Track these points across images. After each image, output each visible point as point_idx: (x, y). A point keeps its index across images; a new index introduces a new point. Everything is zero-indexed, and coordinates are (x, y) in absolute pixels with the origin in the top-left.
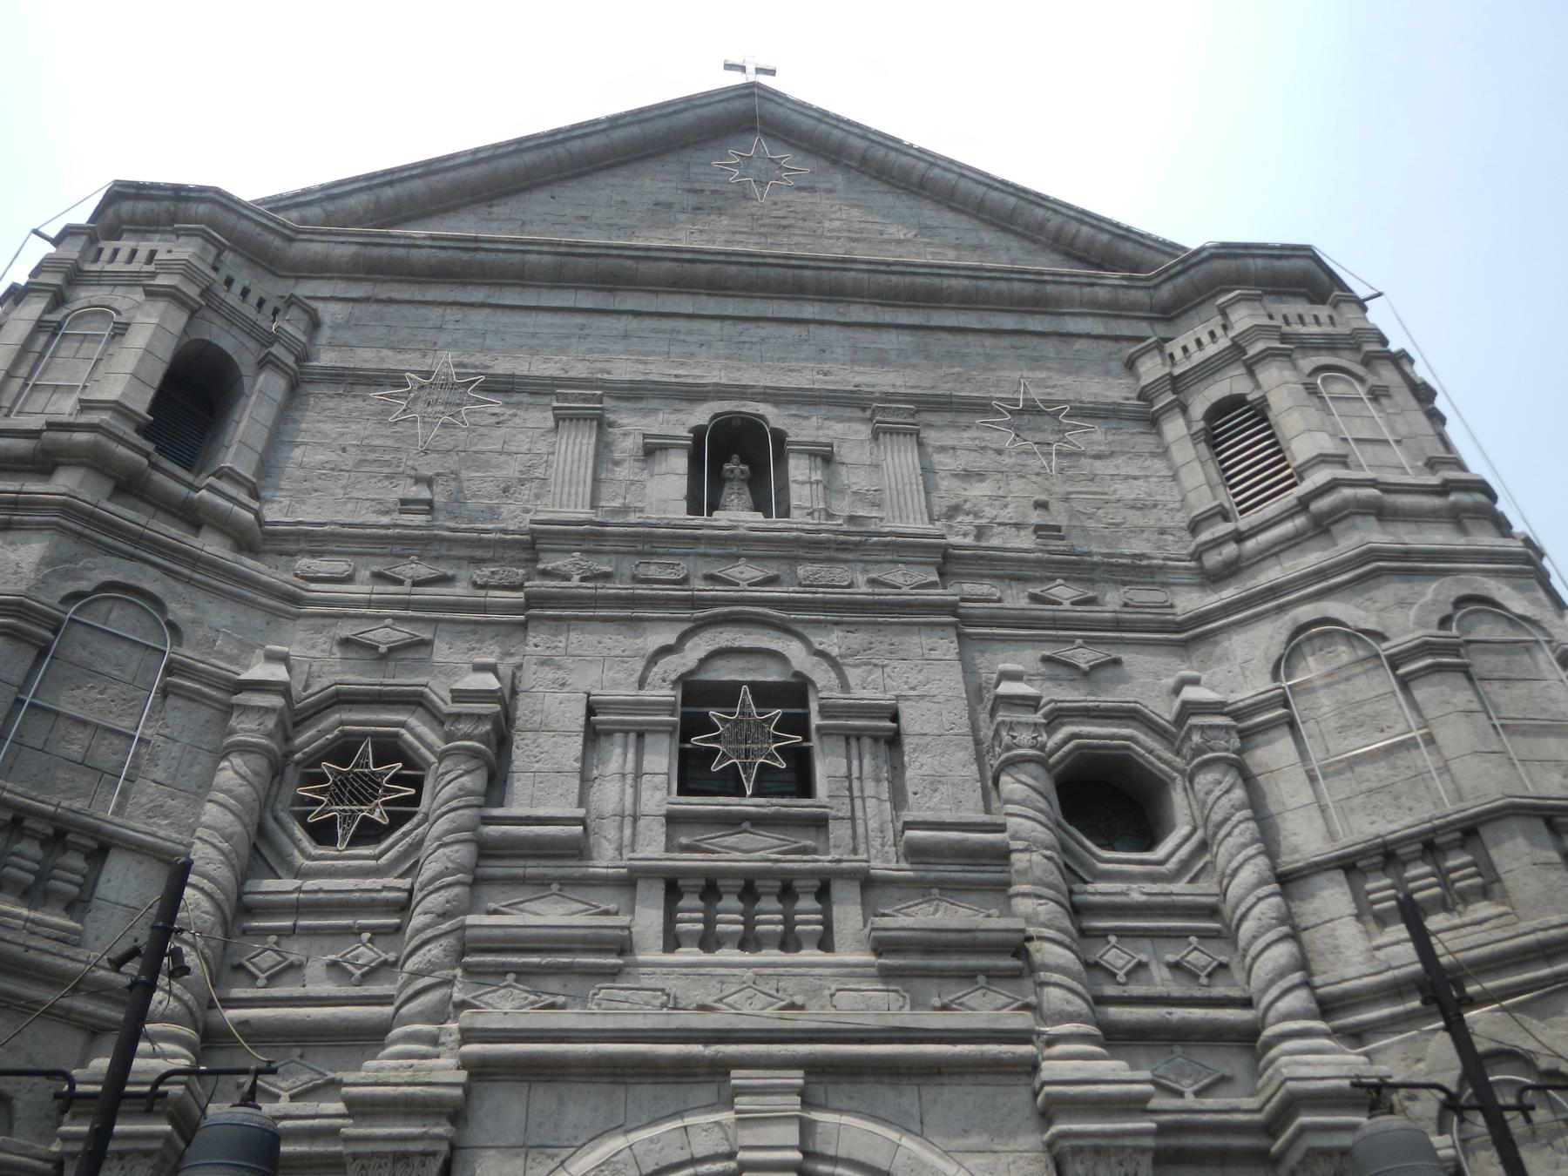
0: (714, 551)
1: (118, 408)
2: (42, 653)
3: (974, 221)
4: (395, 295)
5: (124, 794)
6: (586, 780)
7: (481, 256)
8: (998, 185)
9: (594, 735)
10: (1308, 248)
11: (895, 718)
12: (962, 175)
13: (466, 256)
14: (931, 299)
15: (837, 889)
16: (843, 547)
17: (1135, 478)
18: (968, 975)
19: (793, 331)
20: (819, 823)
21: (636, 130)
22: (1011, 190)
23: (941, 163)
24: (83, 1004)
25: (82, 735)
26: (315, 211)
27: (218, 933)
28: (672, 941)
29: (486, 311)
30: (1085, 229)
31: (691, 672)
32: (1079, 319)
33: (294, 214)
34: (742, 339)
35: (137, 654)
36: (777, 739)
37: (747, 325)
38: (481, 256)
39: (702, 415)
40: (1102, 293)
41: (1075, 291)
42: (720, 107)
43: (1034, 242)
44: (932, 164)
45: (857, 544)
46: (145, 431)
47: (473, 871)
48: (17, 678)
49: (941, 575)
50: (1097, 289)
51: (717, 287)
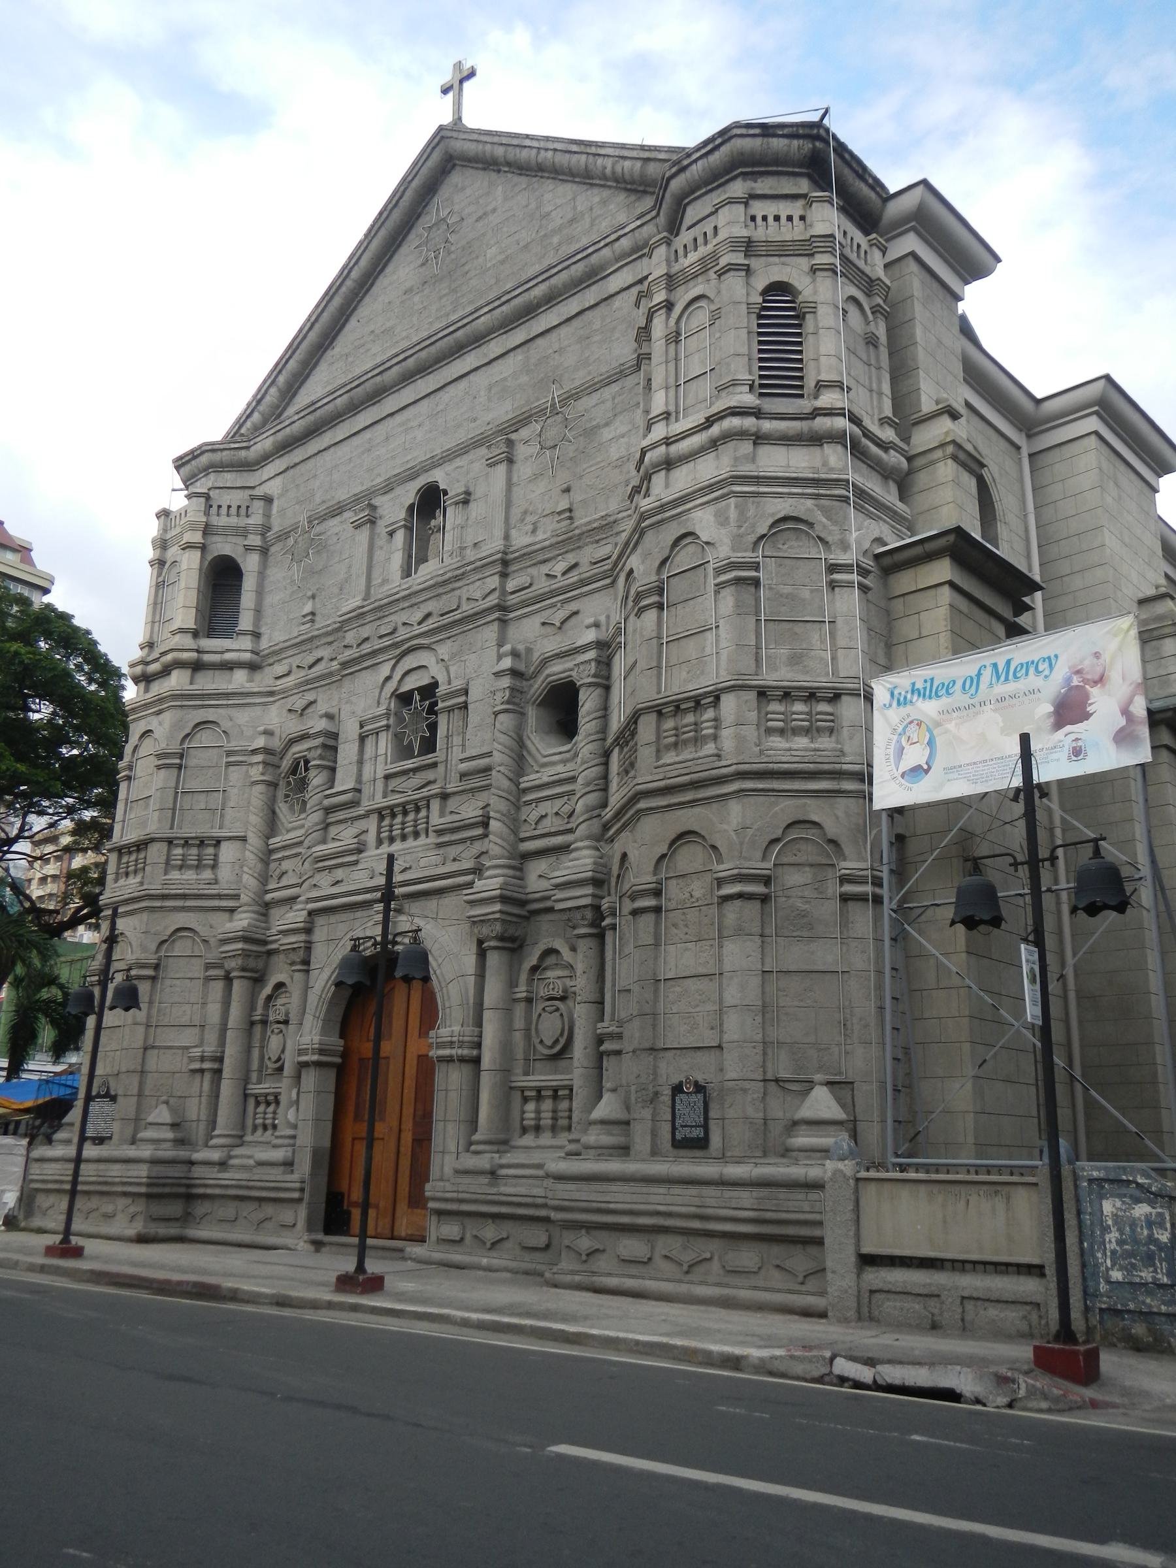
0: (407, 604)
1: (182, 631)
2: (180, 767)
3: (575, 186)
4: (297, 460)
5: (222, 816)
6: (360, 762)
7: (318, 413)
8: (574, 148)
9: (362, 739)
10: (737, 125)
11: (466, 692)
12: (555, 150)
13: (311, 418)
14: (529, 311)
15: (432, 802)
16: (457, 578)
17: (623, 436)
18: (463, 841)
19: (463, 384)
20: (434, 765)
21: (383, 233)
22: (582, 148)
23: (542, 144)
24: (224, 903)
25: (202, 797)
26: (256, 416)
27: (259, 865)
28: (380, 842)
29: (332, 450)
30: (627, 164)
31: (396, 690)
32: (618, 274)
33: (249, 424)
34: (441, 407)
35: (215, 751)
36: (427, 719)
37: (441, 393)
38: (318, 413)
39: (409, 494)
40: (625, 243)
41: (606, 252)
42: (424, 170)
43: (610, 187)
44: (539, 148)
45: (463, 574)
46: (196, 634)
47: (324, 821)
48: (173, 785)
49: (504, 575)
50: (623, 241)
51: (423, 370)
